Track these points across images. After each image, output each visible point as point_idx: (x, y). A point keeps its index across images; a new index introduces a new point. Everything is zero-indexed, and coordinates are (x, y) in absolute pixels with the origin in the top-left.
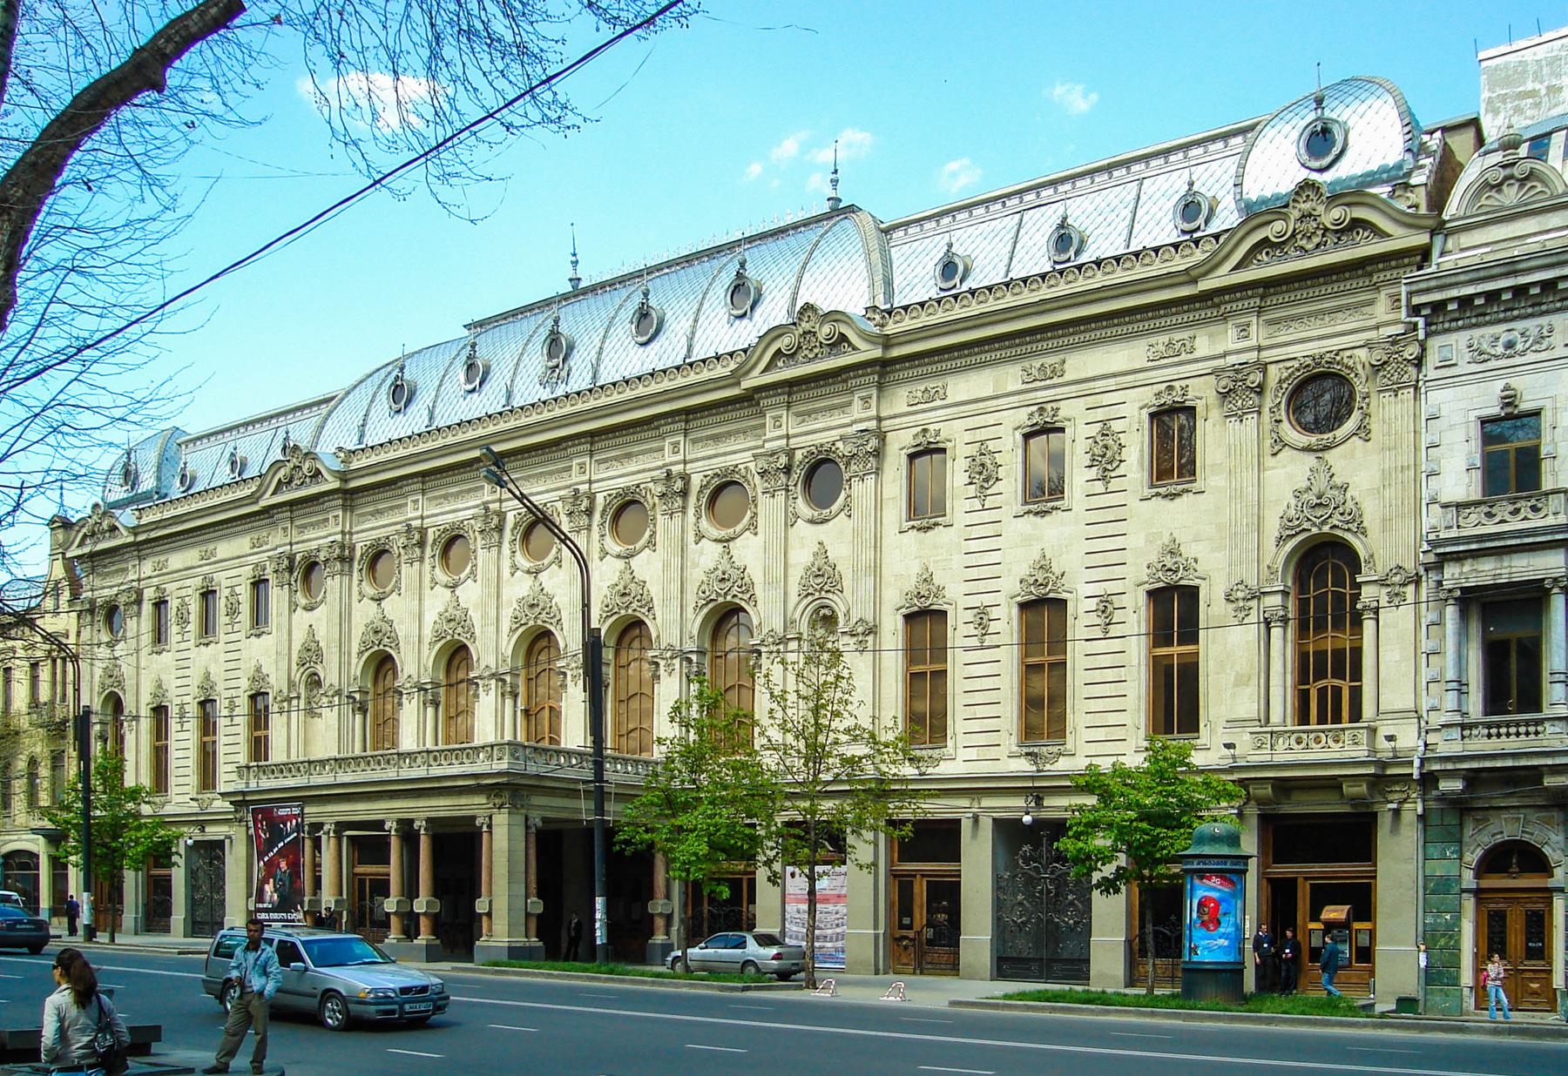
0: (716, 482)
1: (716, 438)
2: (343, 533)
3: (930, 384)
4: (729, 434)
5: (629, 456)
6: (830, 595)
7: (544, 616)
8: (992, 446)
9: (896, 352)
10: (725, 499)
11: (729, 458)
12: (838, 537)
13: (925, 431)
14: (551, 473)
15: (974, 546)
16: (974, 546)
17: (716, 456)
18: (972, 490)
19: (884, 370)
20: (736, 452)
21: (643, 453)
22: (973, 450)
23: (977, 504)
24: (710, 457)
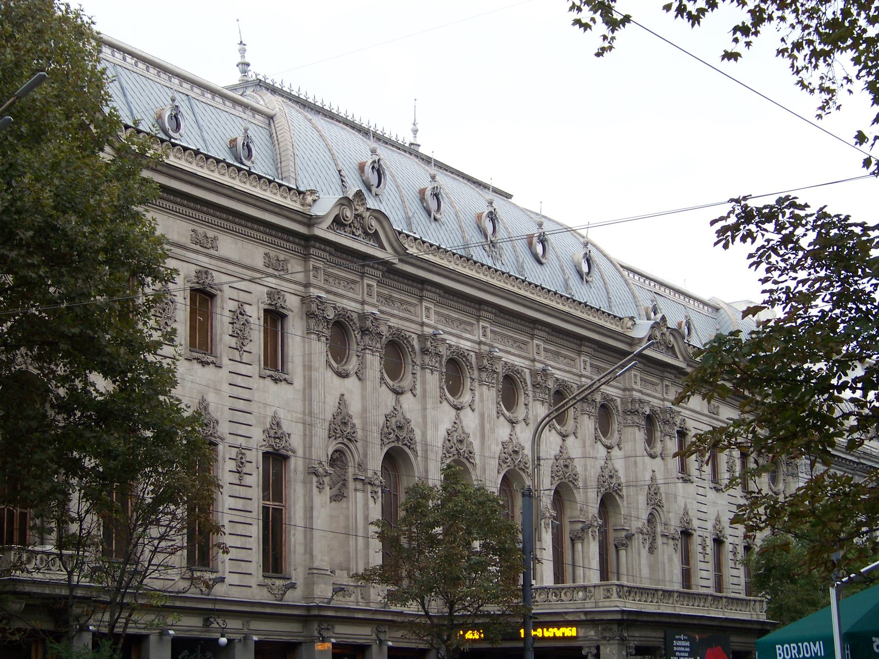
5: (558, 354)
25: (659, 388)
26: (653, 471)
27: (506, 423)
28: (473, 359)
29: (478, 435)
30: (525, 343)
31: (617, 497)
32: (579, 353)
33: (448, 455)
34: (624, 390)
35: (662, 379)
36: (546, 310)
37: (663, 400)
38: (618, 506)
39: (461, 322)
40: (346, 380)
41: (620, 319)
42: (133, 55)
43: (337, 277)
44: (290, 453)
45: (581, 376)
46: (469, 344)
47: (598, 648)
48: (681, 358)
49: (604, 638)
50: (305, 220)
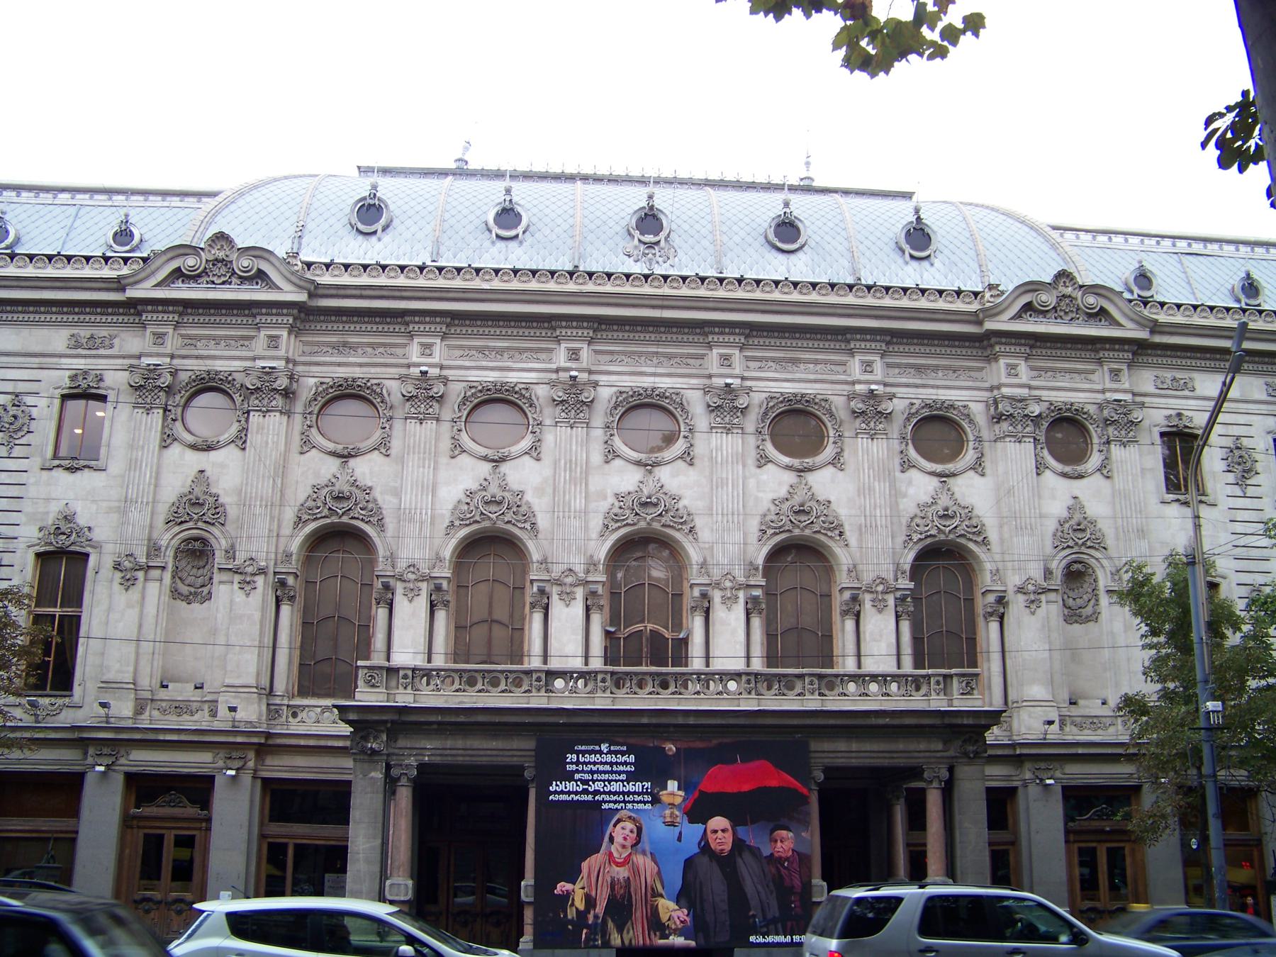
0: (926, 412)
1: (919, 369)
2: (288, 361)
3: (1179, 375)
4: (936, 368)
5: (795, 361)
6: (1097, 554)
7: (666, 519)
8: (1245, 442)
9: (1158, 339)
10: (936, 430)
11: (941, 392)
12: (1094, 496)
13: (1179, 415)
14: (670, 357)
15: (1239, 528)
16: (1239, 528)
17: (924, 386)
18: (1231, 478)
19: (1139, 351)
20: (962, 391)
21: (816, 362)
22: (1229, 442)
23: (1238, 491)
24: (917, 386)
25: (1096, 377)
26: (1075, 498)
27: (632, 467)
28: (542, 392)
29: (550, 490)
30: (702, 357)
31: (971, 546)
32: (851, 353)
33: (457, 523)
34: (991, 389)
35: (1100, 362)
36: (711, 305)
37: (1103, 391)
38: (976, 557)
39: (521, 351)
40: (213, 453)
41: (976, 294)
42: (63, 190)
43: (199, 338)
44: (88, 550)
45: (853, 383)
46: (533, 375)
47: (951, 769)
48: (1129, 325)
49: (966, 754)
50: (115, 285)
